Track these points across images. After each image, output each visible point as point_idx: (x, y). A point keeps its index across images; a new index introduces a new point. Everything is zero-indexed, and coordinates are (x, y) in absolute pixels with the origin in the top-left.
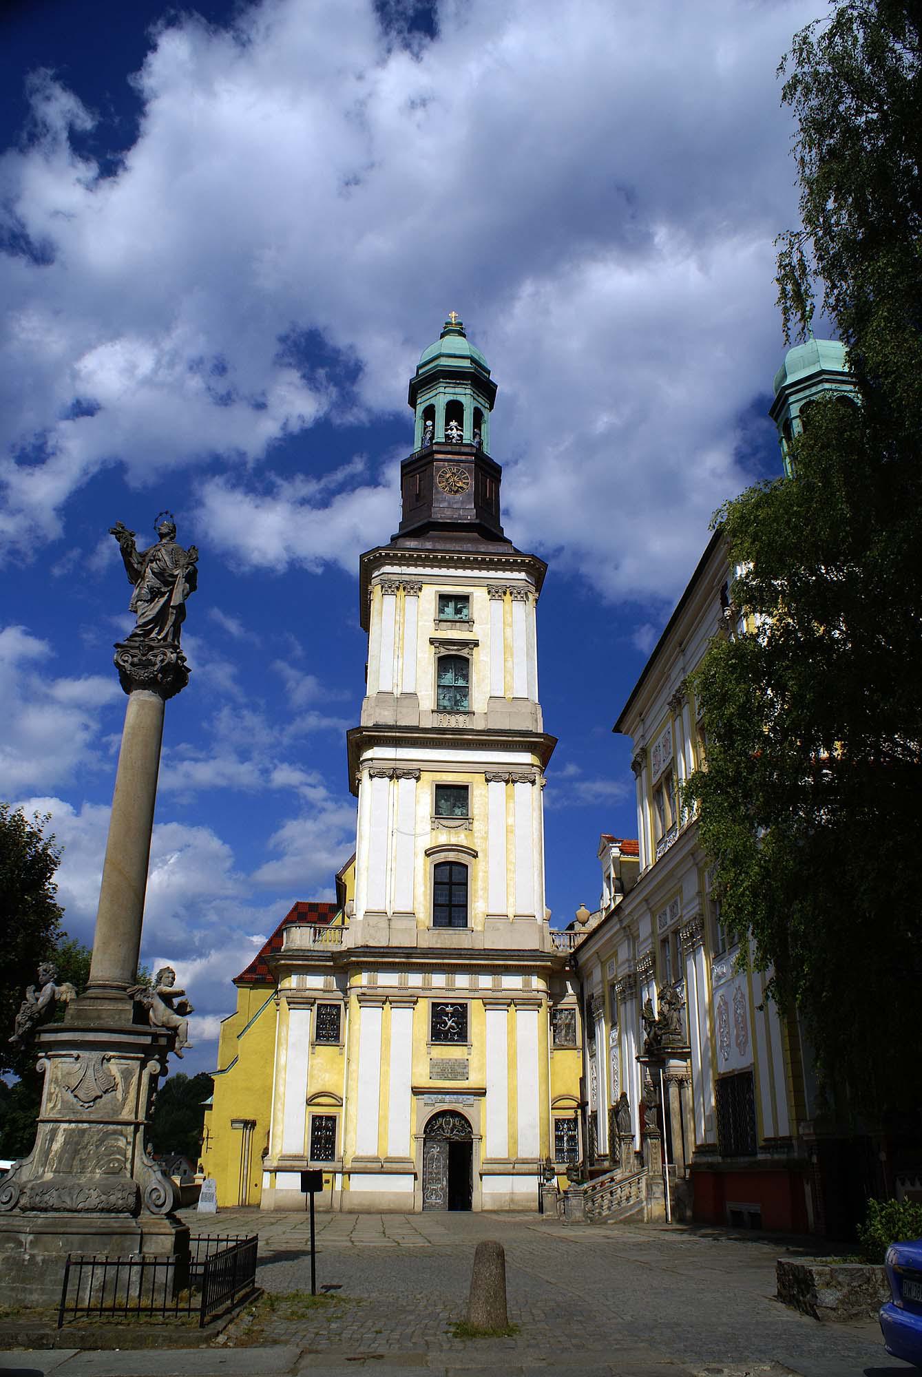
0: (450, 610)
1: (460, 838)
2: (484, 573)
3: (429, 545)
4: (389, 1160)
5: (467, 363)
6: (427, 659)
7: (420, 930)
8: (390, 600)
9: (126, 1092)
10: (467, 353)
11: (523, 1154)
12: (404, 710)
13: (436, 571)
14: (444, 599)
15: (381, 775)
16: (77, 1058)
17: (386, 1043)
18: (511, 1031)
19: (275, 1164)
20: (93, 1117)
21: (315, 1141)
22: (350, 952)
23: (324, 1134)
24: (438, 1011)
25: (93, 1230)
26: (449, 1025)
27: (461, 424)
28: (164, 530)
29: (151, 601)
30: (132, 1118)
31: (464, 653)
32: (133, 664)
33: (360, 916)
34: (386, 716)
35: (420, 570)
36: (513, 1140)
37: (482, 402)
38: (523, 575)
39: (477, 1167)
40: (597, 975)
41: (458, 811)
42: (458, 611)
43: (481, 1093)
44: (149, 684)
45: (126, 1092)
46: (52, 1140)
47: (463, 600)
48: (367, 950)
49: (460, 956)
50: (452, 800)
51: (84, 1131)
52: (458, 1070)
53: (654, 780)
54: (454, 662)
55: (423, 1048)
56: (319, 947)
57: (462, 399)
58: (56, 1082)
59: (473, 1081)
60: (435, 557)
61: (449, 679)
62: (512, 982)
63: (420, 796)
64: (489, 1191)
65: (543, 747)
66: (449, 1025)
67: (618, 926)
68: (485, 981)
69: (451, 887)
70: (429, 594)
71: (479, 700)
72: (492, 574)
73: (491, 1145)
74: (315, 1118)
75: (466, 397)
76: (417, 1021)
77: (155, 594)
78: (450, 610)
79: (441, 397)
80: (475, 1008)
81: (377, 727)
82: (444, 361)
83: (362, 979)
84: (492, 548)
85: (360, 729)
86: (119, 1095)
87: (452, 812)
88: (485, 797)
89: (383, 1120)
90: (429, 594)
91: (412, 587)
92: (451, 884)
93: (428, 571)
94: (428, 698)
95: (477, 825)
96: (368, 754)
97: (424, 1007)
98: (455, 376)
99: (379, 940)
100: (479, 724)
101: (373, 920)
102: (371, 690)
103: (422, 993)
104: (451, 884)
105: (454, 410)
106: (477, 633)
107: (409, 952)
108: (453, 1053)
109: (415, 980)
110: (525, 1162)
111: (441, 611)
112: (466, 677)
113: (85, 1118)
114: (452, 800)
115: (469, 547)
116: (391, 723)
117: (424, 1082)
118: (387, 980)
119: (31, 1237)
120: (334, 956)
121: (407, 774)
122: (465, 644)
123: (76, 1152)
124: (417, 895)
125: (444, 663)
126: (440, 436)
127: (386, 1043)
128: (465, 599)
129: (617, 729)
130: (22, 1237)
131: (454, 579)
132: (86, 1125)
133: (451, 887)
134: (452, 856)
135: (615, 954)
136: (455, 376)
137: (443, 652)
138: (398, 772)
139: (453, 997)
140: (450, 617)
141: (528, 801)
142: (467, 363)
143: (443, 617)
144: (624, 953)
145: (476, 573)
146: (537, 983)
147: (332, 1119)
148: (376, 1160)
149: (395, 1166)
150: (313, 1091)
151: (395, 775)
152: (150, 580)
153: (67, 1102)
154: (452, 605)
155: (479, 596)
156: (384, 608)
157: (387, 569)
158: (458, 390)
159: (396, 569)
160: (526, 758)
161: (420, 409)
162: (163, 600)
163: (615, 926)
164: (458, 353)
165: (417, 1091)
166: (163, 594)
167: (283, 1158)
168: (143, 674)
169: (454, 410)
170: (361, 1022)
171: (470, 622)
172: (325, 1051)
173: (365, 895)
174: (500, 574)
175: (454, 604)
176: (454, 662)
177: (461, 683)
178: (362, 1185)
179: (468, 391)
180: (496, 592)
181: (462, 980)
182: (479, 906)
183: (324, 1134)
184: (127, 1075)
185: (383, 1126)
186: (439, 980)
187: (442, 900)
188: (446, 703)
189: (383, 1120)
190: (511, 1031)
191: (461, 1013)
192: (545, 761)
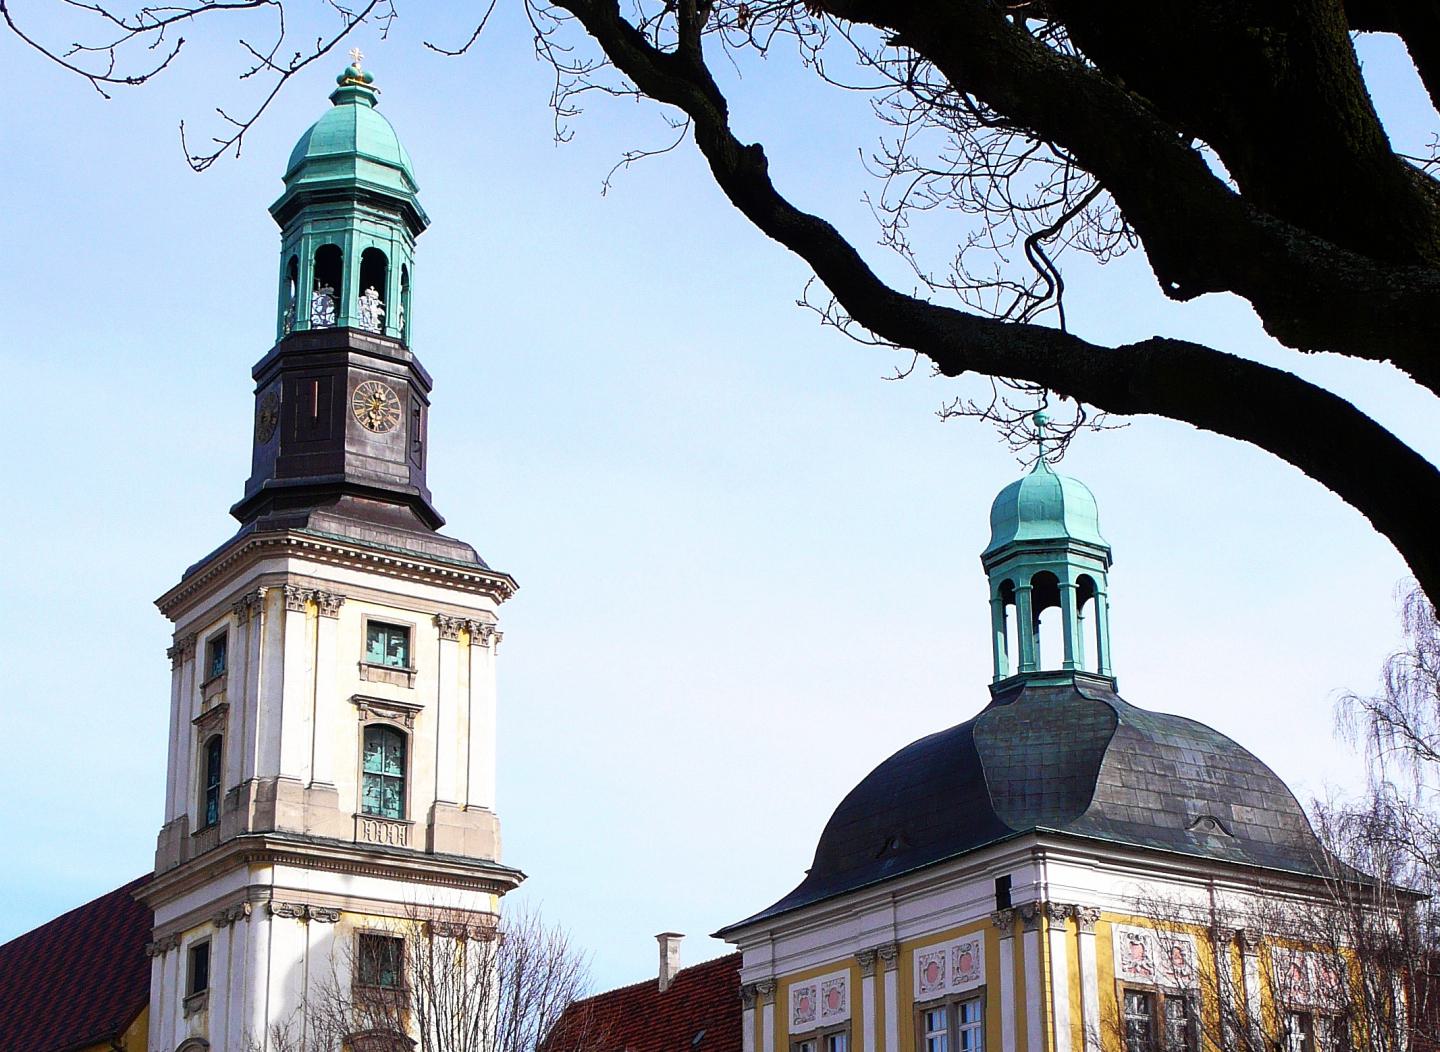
0: (379, 647)
6: (348, 727)
10: (395, 160)
12: (319, 812)
14: (375, 627)
15: (288, 912)
31: (400, 723)
42: (392, 651)
47: (404, 632)
53: (795, 1029)
54: (387, 737)
57: (384, 247)
60: (370, 558)
70: (352, 617)
78: (379, 647)
90: (352, 617)
94: (351, 795)
100: (418, 843)
106: (419, 693)
111: (370, 648)
112: (403, 763)
116: (300, 830)
122: (409, 710)
128: (404, 632)
137: (373, 720)
138: (311, 910)
140: (378, 660)
143: (369, 658)
158: (382, 230)
164: (384, 157)
171: (408, 670)
176: (387, 737)
177: (394, 771)
179: (396, 236)
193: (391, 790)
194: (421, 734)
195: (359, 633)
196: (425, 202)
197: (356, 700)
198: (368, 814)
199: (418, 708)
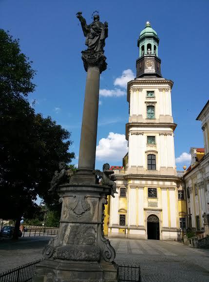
0: (149, 95)
1: (153, 149)
2: (157, 85)
3: (144, 79)
4: (139, 226)
5: (152, 34)
6: (145, 106)
7: (144, 170)
8: (135, 93)
9: (94, 210)
11: (172, 226)
13: (146, 85)
14: (148, 92)
15: (134, 134)
16: (75, 197)
17: (137, 198)
18: (168, 196)
19: (111, 226)
20: (81, 221)
21: (121, 221)
22: (128, 176)
23: (123, 219)
24: (150, 190)
25: (83, 270)
26: (152, 193)
27: (151, 49)
28: (96, 17)
29: (93, 38)
30: (96, 221)
31: (153, 105)
32: (88, 58)
33: (130, 167)
34: (134, 120)
35: (142, 85)
36: (170, 222)
37: (156, 44)
38: (167, 85)
39: (160, 230)
40: (190, 182)
41: (153, 143)
42: (151, 95)
43: (161, 210)
44: (93, 65)
45: (94, 210)
46: (65, 230)
48: (132, 175)
49: (155, 177)
50: (151, 139)
51: (78, 227)
52: (155, 204)
54: (151, 107)
55: (146, 198)
56: (121, 174)
58: (67, 207)
59: (159, 207)
61: (150, 111)
62: (168, 184)
63: (144, 138)
64: (164, 235)
65: (174, 127)
66: (152, 193)
67: (198, 169)
68: (161, 183)
69: (152, 160)
71: (157, 116)
72: (159, 85)
73: (164, 223)
74: (120, 215)
75: (152, 42)
76: (145, 192)
77: (94, 36)
78: (149, 95)
79: (146, 43)
80: (159, 190)
81: (133, 123)
82: (146, 34)
83: (131, 182)
84: (159, 79)
85: (129, 123)
86: (91, 211)
87: (151, 142)
88: (158, 138)
89: (137, 216)
90: (144, 91)
91: (140, 90)
92: (151, 159)
93: (144, 85)
94: (145, 116)
95: (157, 146)
96: (131, 129)
97: (146, 189)
98: (149, 37)
99: (135, 173)
100: (157, 121)
101: (133, 168)
102: (131, 114)
103: (145, 185)
104: (151, 159)
105: (149, 46)
107: (142, 176)
108: (153, 200)
109: (144, 182)
110: (173, 228)
112: (154, 111)
113: (78, 221)
114: (151, 139)
115: (154, 79)
117: (146, 207)
118: (137, 182)
119: (58, 271)
120: (124, 177)
121: (140, 134)
123: (75, 235)
124: (144, 163)
125: (148, 107)
126: (146, 52)
127: (137, 198)
128: (153, 92)
129: (197, 119)
130: (54, 271)
131: (150, 87)
132: (78, 224)
133: (152, 160)
134: (151, 153)
135: (196, 177)
136: (149, 37)
139: (153, 187)
141: (170, 139)
142: (152, 34)
144: (199, 176)
145: (155, 85)
146: (174, 184)
147: (124, 215)
148: (136, 226)
149: (140, 228)
150: (120, 208)
151: (137, 134)
152: (92, 31)
153: (71, 214)
154: (150, 93)
155: (157, 91)
156: (134, 95)
157: (134, 85)
158: (150, 41)
159: (136, 85)
160: (170, 129)
161: (140, 47)
162: (98, 37)
163: (197, 169)
165: (145, 209)
166: (97, 36)
167: (113, 225)
168: (93, 61)
169: (149, 46)
170: (131, 192)
172: (122, 199)
173: (131, 163)
174: (161, 85)
175: (151, 93)
176: (151, 107)
178: (133, 233)
180: (161, 90)
181: (155, 183)
182: (159, 164)
183: (123, 219)
184: (94, 204)
185: (138, 218)
186: (149, 182)
187: (150, 163)
188: (150, 117)
189: (137, 216)
190: (168, 196)
191: (155, 190)
192: (174, 130)
193: (151, 115)
194: (157, 106)
195: (146, 93)
196: (159, 37)
197: (145, 102)
198: (148, 119)
199: (156, 102)
